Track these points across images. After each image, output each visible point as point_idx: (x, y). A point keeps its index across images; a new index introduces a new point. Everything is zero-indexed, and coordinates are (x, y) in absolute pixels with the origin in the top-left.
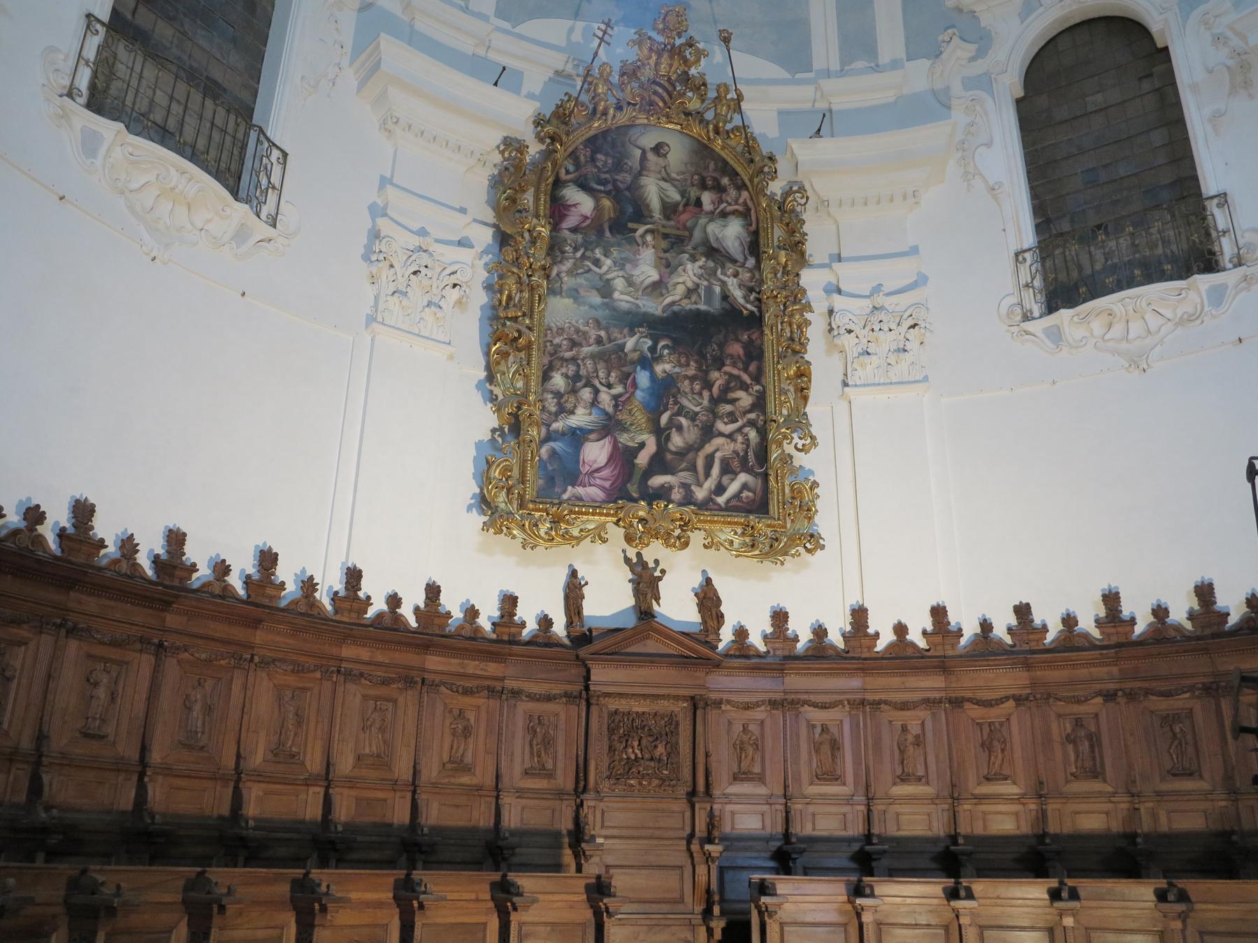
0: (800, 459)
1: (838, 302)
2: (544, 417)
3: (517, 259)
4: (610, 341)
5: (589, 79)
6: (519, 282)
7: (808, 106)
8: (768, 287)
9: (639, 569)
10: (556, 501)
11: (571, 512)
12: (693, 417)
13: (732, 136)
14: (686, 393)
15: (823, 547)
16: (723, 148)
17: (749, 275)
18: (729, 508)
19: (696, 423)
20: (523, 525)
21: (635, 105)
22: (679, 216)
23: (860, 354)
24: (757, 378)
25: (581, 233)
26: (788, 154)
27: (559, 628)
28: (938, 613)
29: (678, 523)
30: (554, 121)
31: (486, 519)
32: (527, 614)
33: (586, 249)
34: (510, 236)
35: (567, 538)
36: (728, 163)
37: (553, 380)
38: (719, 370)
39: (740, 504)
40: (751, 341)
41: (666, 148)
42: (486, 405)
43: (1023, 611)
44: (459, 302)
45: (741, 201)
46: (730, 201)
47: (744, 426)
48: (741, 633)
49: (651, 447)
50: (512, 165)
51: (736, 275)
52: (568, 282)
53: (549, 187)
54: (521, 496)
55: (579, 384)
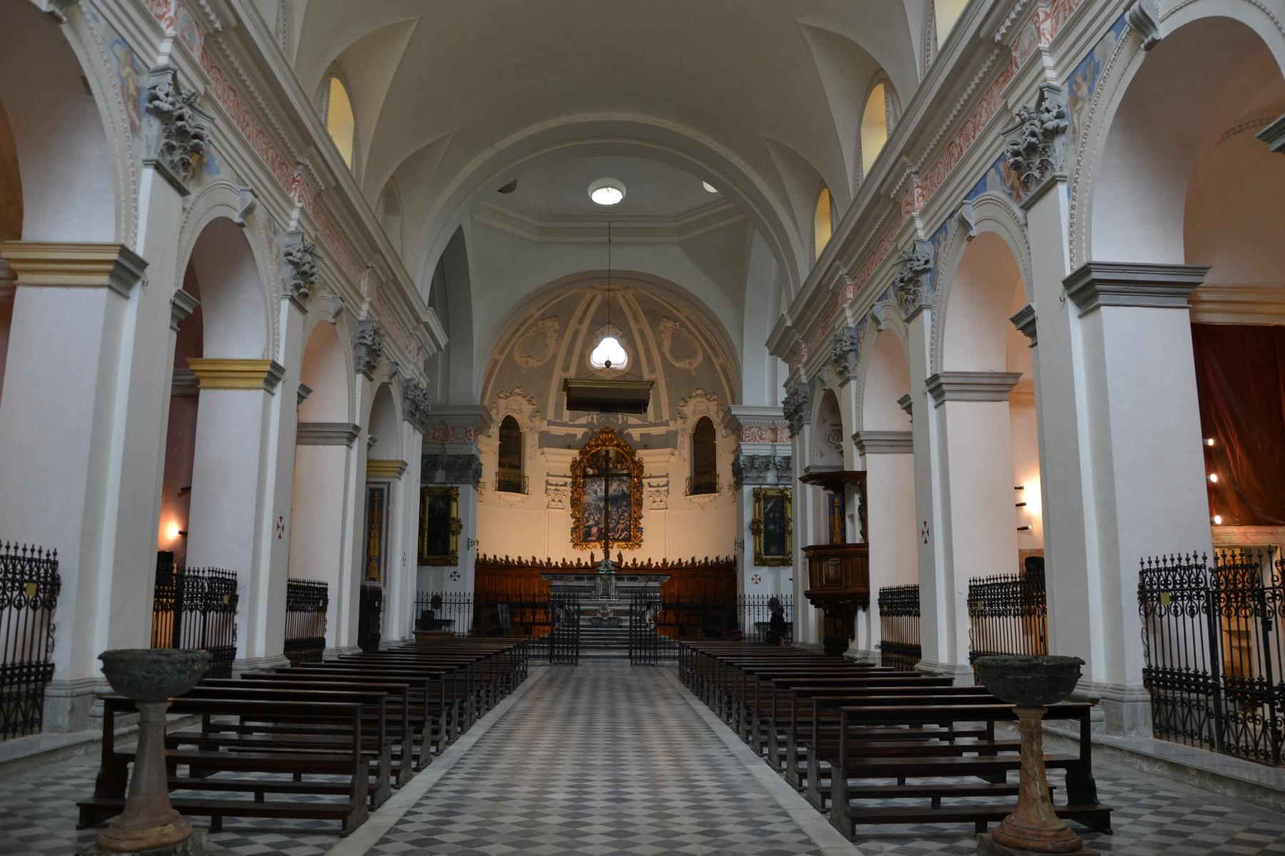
27: (589, 564)
28: (664, 560)
43: (680, 560)
48: (626, 563)
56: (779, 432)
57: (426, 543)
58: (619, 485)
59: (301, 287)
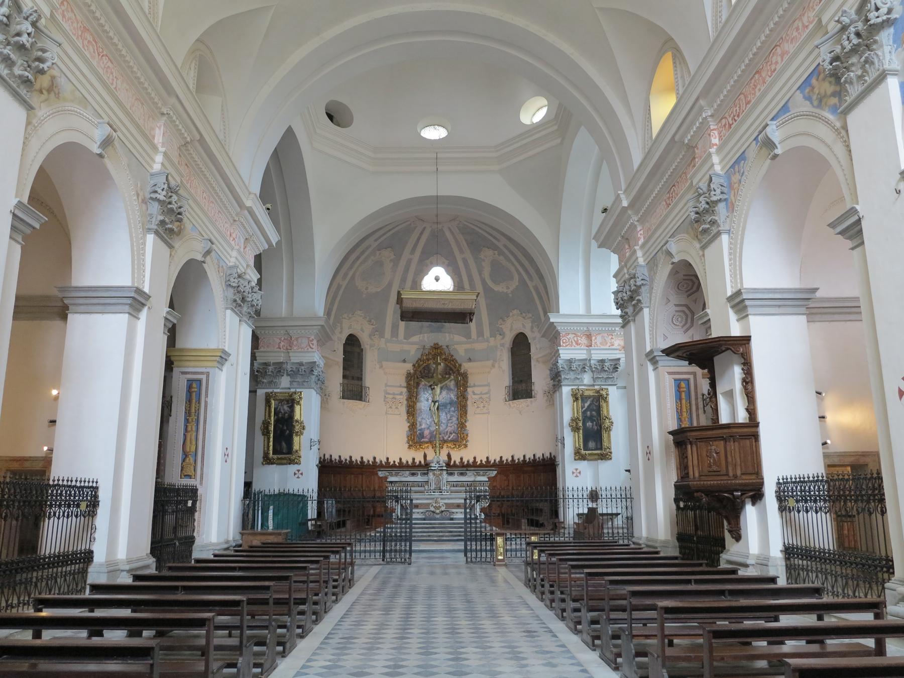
27: (423, 462)
28: (487, 458)
32: (417, 461)
48: (455, 462)
56: (593, 338)
57: (271, 444)
58: (447, 393)
59: (167, 224)
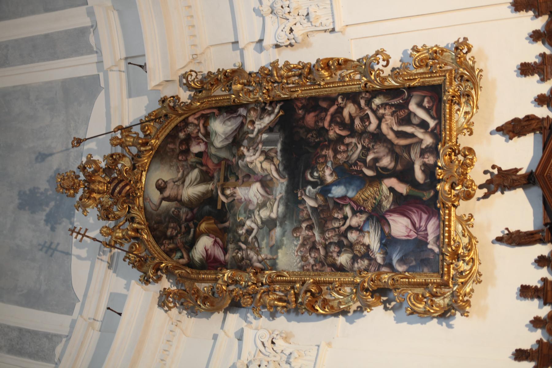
0: (395, 62)
1: (269, 41)
2: (373, 269)
3: (250, 294)
4: (309, 219)
5: (113, 243)
6: (268, 292)
7: (124, 75)
8: (261, 96)
9: (492, 187)
10: (441, 257)
11: (449, 245)
12: (366, 150)
13: (149, 132)
14: (348, 156)
15: (466, 39)
16: (158, 138)
17: (252, 112)
18: (438, 115)
19: (371, 147)
20: (462, 283)
21: (129, 208)
22: (210, 169)
23: (309, 20)
24: (332, 100)
25: (227, 245)
26: (160, 88)
29: (453, 157)
30: (145, 268)
31: (458, 314)
33: (240, 240)
34: (233, 300)
35: (469, 248)
36: (168, 134)
37: (343, 263)
38: (327, 131)
39: (434, 108)
40: (303, 107)
41: (160, 182)
42: (365, 315)
44: (286, 339)
45: (196, 122)
46: (196, 131)
47: (371, 109)
49: (392, 182)
50: (179, 300)
51: (253, 122)
52: (265, 254)
53: (194, 271)
54: (439, 285)
55: (345, 242)
58: (253, 143)
